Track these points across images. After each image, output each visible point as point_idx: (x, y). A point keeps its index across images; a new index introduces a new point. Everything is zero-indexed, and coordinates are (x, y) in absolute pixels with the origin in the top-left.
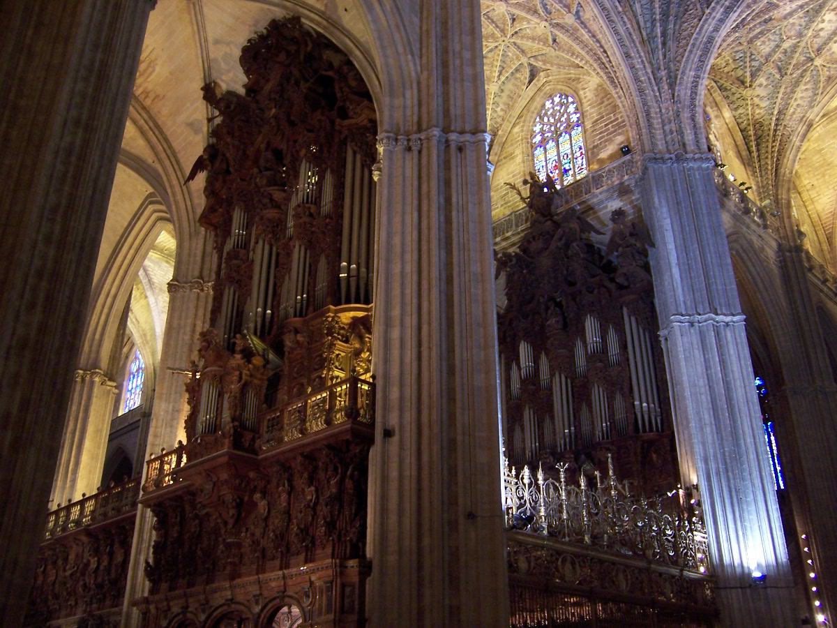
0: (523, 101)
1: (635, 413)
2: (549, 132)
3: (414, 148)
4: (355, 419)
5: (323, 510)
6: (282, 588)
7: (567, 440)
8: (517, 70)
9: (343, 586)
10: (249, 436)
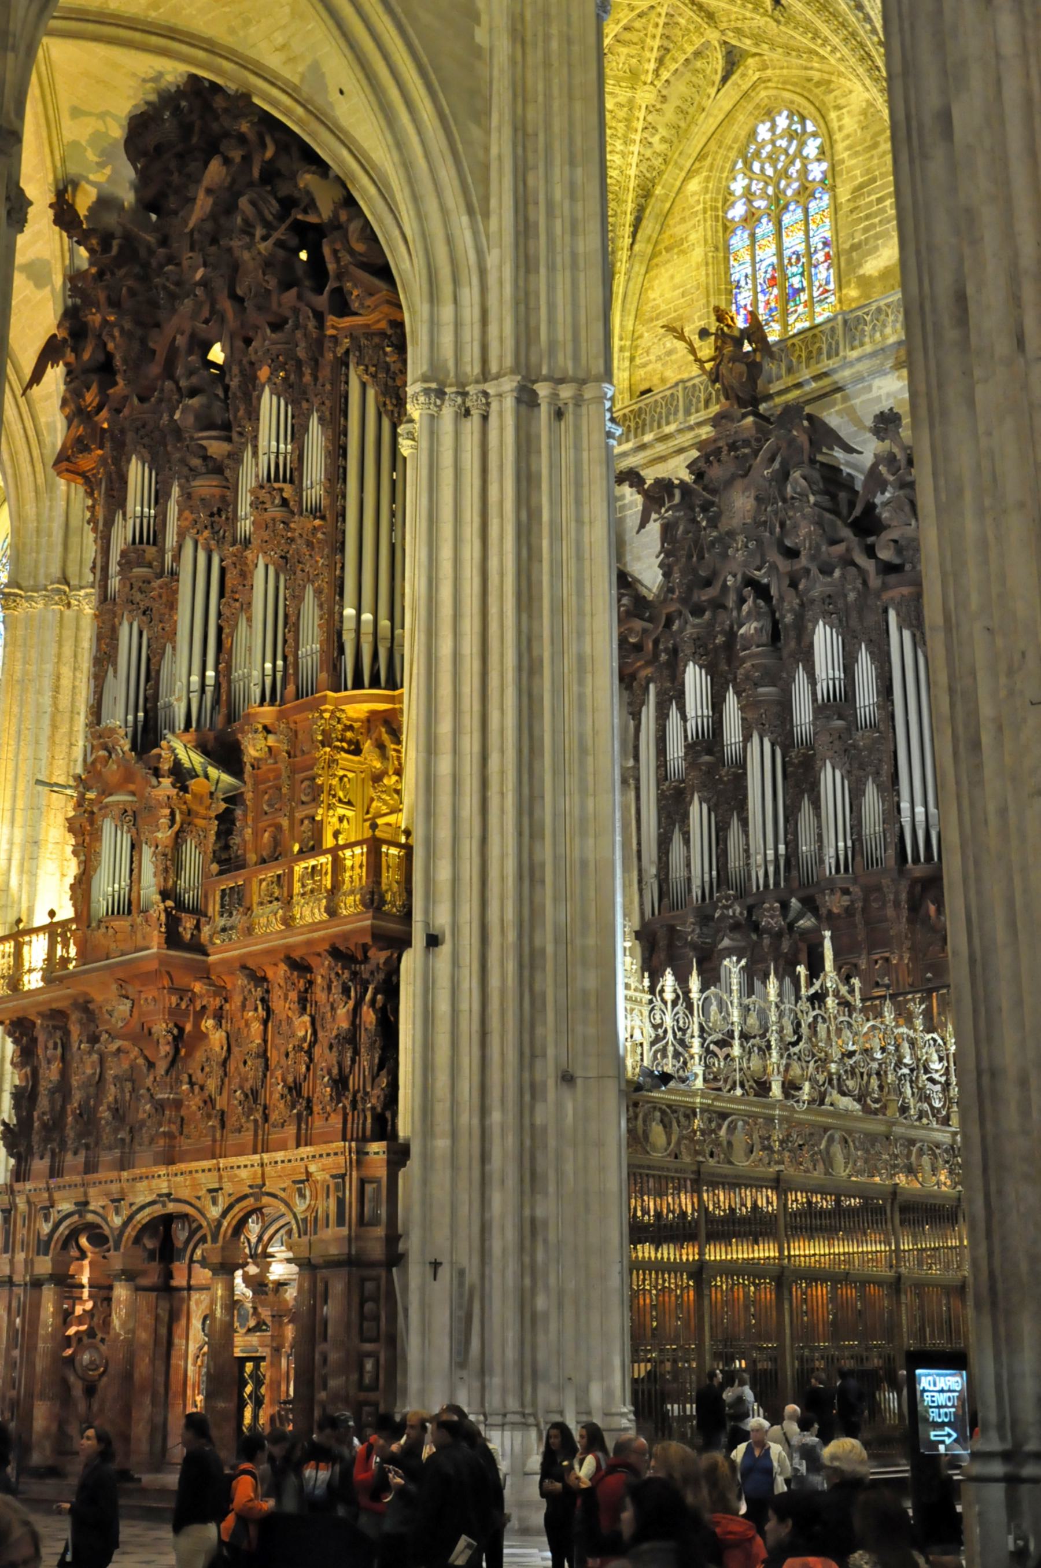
0: (711, 120)
1: (901, 828)
2: (762, 198)
3: (474, 412)
4: (378, 909)
5: (325, 1057)
6: (259, 1182)
7: (771, 869)
8: (698, 54)
9: (362, 1182)
10: (188, 923)
